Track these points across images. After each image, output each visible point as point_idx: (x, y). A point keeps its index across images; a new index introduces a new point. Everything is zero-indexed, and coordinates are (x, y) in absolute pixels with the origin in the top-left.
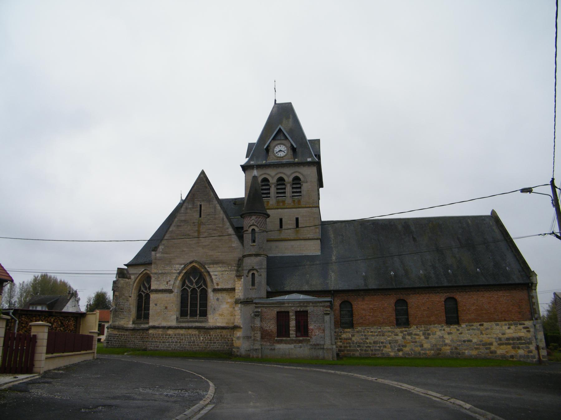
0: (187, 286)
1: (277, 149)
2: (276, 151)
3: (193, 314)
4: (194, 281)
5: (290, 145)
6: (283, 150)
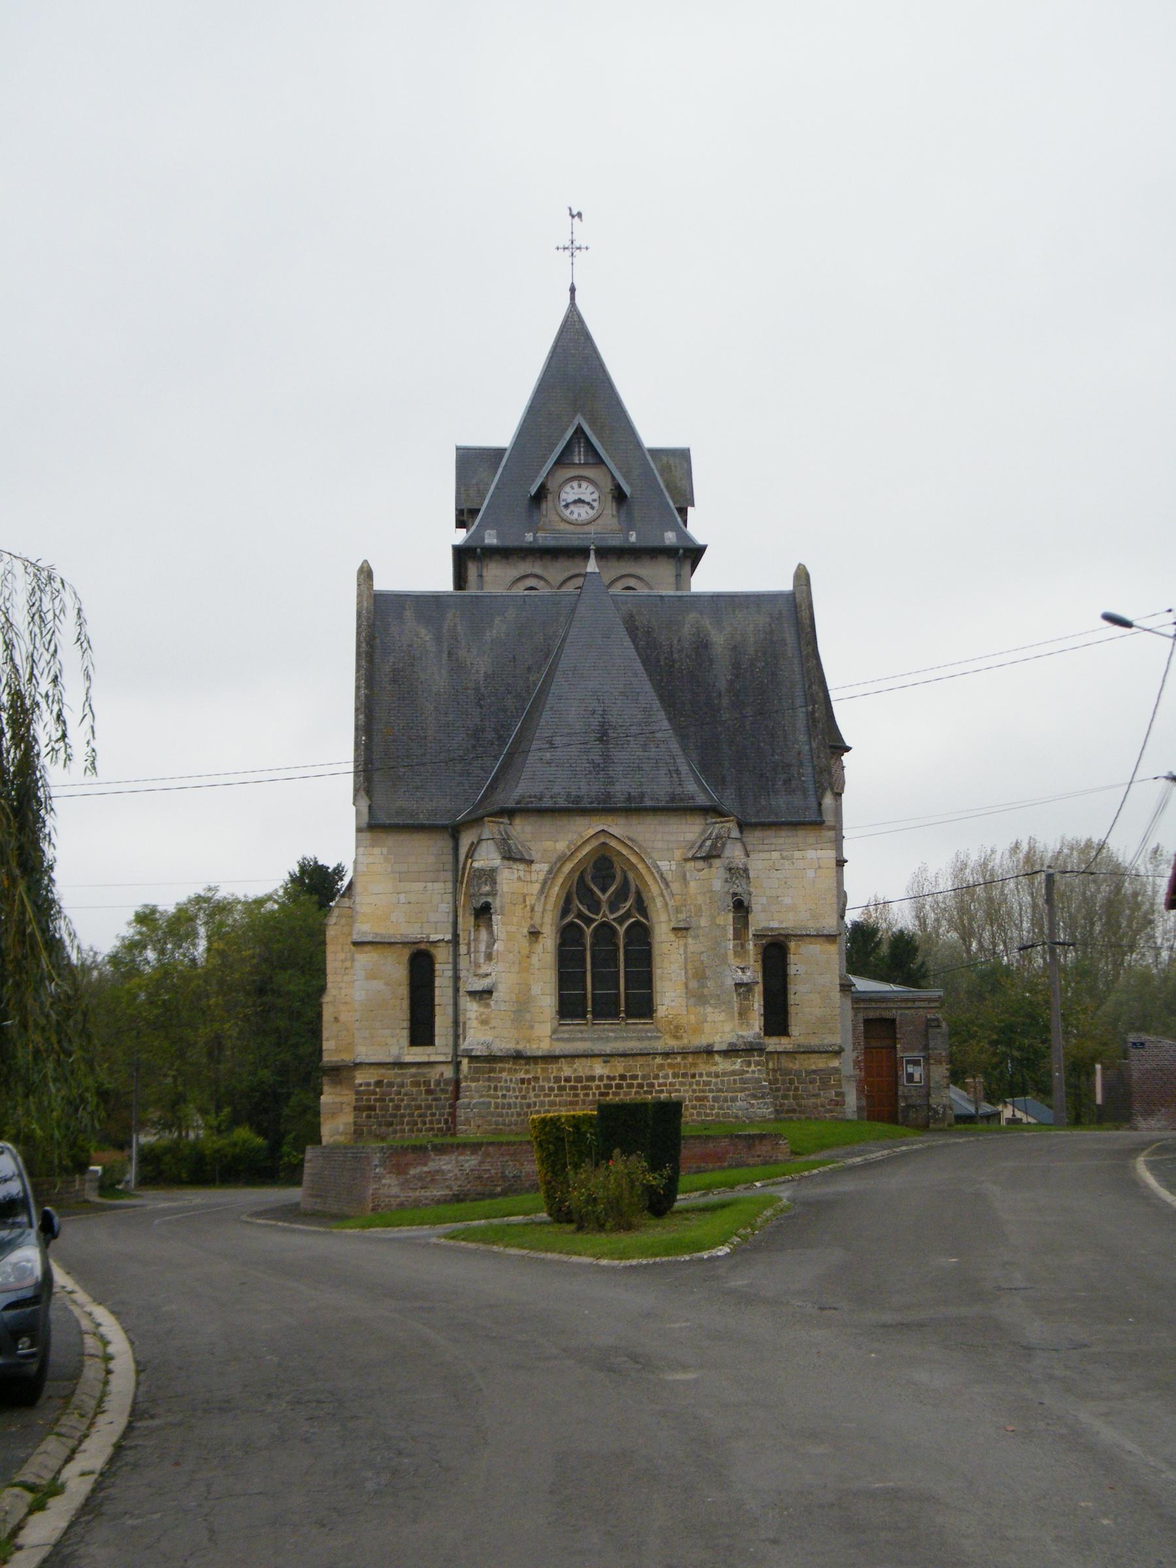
0: (580, 915)
1: (570, 493)
2: (563, 501)
3: (606, 1009)
4: (604, 897)
5: (608, 486)
6: (587, 498)
